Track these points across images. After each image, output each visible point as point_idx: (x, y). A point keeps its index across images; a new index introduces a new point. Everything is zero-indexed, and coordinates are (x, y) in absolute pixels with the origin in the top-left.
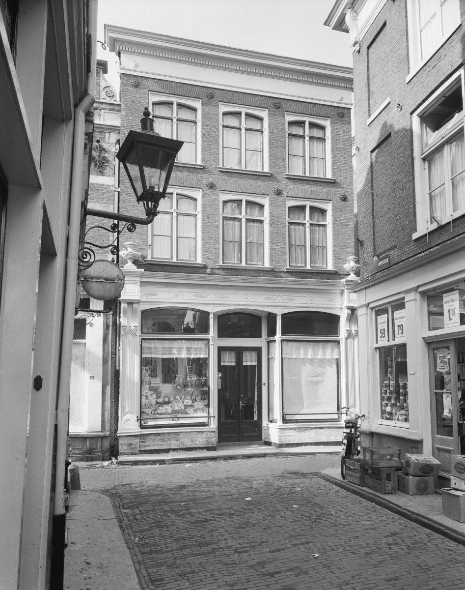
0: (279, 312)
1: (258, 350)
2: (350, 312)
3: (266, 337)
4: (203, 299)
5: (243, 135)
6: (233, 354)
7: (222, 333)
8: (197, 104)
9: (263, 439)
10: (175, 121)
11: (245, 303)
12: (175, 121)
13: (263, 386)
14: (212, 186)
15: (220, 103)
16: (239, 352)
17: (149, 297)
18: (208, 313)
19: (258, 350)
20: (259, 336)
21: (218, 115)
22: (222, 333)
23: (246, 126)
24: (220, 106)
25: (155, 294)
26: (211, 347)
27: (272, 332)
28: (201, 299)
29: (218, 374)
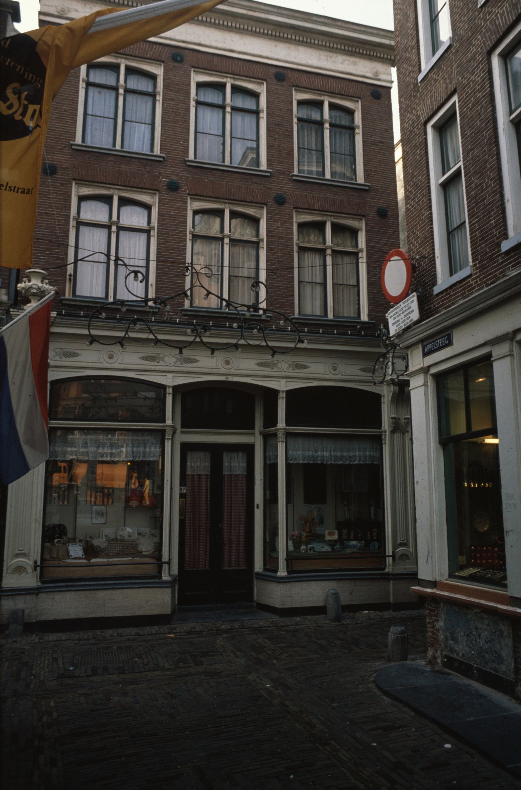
0: (282, 386)
1: (248, 450)
2: (397, 389)
3: (262, 428)
4: (155, 363)
5: (228, 117)
6: (208, 455)
7: (189, 421)
8: (159, 71)
9: (255, 599)
10: (121, 91)
11: (223, 371)
12: (121, 91)
13: (256, 510)
14: (173, 187)
15: (192, 70)
16: (216, 452)
17: (64, 359)
18: (163, 387)
19: (248, 450)
20: (251, 426)
21: (189, 85)
22: (189, 421)
23: (232, 104)
24: (192, 74)
25: (75, 355)
26: (168, 445)
27: (271, 419)
28: (152, 363)
29: (180, 489)
